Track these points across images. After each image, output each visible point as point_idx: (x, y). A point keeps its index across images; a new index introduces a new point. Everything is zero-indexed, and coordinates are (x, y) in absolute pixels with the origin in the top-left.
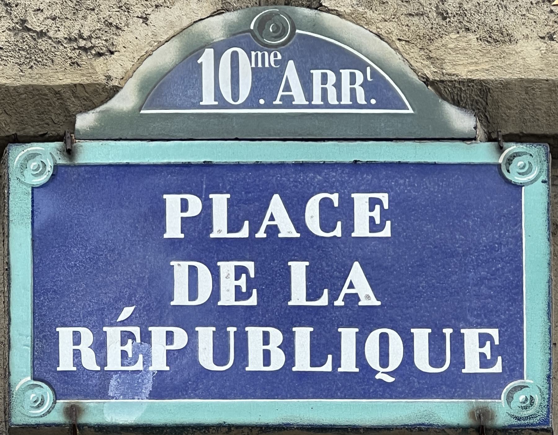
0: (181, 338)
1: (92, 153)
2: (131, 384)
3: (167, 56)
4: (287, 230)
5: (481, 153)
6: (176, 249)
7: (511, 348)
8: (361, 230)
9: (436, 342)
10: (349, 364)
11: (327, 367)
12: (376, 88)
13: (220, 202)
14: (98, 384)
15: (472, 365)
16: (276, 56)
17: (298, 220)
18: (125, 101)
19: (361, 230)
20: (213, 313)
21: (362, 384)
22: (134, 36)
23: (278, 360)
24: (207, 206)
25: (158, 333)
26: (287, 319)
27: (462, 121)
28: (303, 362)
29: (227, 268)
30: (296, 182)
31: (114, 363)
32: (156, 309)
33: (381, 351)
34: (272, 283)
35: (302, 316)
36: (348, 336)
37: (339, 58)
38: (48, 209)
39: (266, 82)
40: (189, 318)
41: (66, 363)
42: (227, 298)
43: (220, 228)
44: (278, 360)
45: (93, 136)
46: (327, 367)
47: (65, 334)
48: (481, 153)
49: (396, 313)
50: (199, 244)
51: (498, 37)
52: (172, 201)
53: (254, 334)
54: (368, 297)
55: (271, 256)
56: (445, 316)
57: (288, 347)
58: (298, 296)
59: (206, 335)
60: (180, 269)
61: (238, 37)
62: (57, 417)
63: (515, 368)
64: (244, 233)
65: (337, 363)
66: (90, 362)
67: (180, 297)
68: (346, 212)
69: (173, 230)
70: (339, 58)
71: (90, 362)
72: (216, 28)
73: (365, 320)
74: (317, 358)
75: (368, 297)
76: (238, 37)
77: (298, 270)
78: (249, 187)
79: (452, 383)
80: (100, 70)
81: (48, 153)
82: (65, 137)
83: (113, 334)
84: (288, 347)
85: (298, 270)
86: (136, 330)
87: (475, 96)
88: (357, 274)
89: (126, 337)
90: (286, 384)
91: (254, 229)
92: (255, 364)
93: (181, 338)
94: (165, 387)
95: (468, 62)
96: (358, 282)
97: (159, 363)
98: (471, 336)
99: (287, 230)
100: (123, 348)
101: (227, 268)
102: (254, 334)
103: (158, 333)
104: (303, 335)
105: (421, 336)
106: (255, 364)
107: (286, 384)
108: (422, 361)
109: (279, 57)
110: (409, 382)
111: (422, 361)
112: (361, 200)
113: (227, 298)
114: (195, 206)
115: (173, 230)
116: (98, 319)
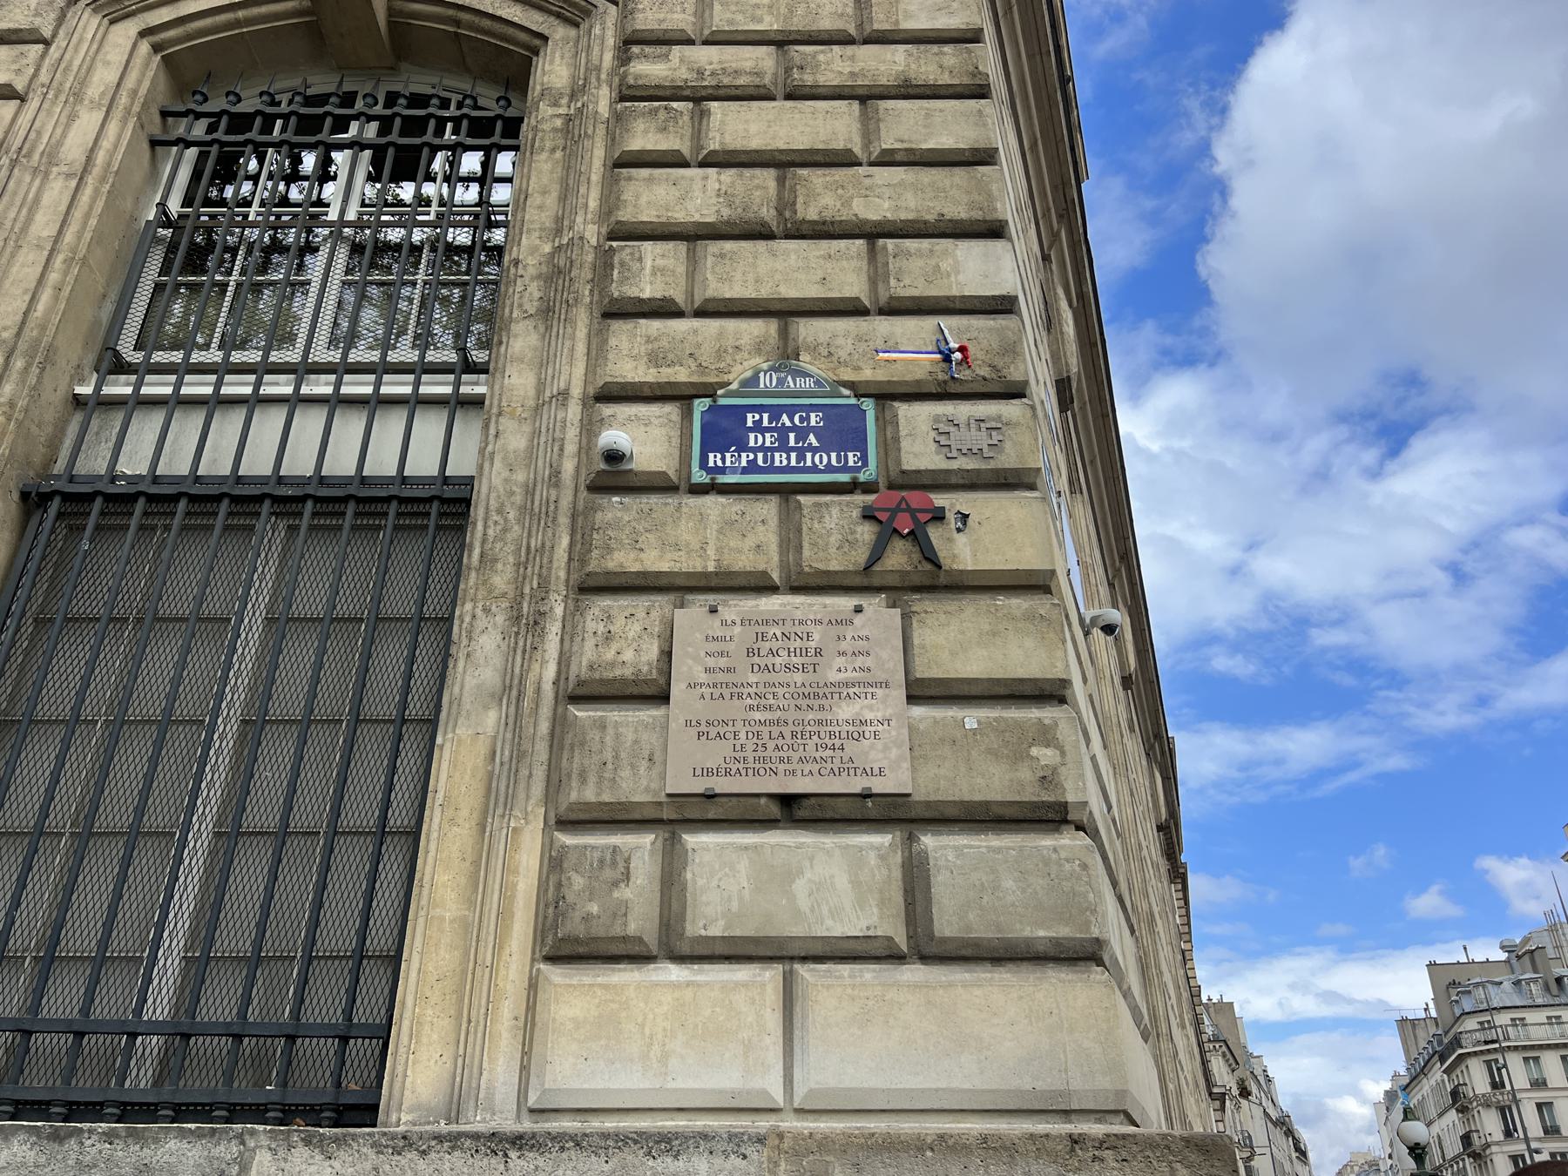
0: (752, 456)
1: (722, 402)
2: (734, 470)
3: (749, 374)
4: (788, 424)
5: (853, 401)
6: (751, 430)
7: (864, 459)
8: (813, 423)
9: (839, 457)
10: (809, 463)
12: (817, 383)
13: (766, 416)
14: (722, 470)
15: (851, 463)
17: (792, 420)
18: (734, 386)
19: (813, 423)
20: (763, 449)
21: (814, 469)
22: (737, 368)
23: (785, 463)
25: (744, 455)
26: (788, 450)
27: (846, 392)
28: (793, 463)
29: (768, 435)
30: (791, 410)
31: (728, 464)
32: (743, 447)
33: (821, 459)
35: (793, 449)
36: (809, 455)
37: (806, 375)
38: (707, 417)
39: (781, 382)
40: (755, 450)
41: (711, 464)
42: (768, 444)
43: (765, 423)
44: (785, 463)
45: (723, 396)
47: (711, 455)
48: (853, 401)
49: (825, 448)
50: (758, 427)
51: (857, 368)
52: (749, 416)
53: (777, 455)
54: (815, 443)
55: (783, 432)
56: (842, 448)
57: (788, 458)
58: (792, 443)
59: (760, 455)
60: (752, 436)
61: (772, 369)
62: (707, 481)
63: (865, 464)
66: (720, 464)
67: (752, 444)
68: (808, 418)
69: (750, 424)
70: (806, 375)
71: (720, 464)
72: (765, 366)
73: (814, 450)
75: (815, 443)
76: (772, 369)
77: (792, 436)
78: (775, 412)
79: (845, 469)
80: (726, 378)
81: (708, 401)
82: (713, 396)
83: (728, 455)
84: (788, 458)
85: (792, 436)
87: (850, 385)
88: (812, 436)
90: (788, 469)
92: (777, 464)
94: (745, 471)
95: (847, 375)
96: (812, 439)
97: (744, 463)
98: (850, 455)
99: (788, 424)
101: (768, 435)
102: (777, 455)
103: (744, 455)
104: (793, 455)
105: (834, 455)
106: (777, 464)
107: (788, 469)
108: (834, 462)
110: (829, 469)
111: (834, 462)
112: (813, 415)
113: (768, 444)
114: (757, 417)
115: (750, 424)
116: (723, 450)
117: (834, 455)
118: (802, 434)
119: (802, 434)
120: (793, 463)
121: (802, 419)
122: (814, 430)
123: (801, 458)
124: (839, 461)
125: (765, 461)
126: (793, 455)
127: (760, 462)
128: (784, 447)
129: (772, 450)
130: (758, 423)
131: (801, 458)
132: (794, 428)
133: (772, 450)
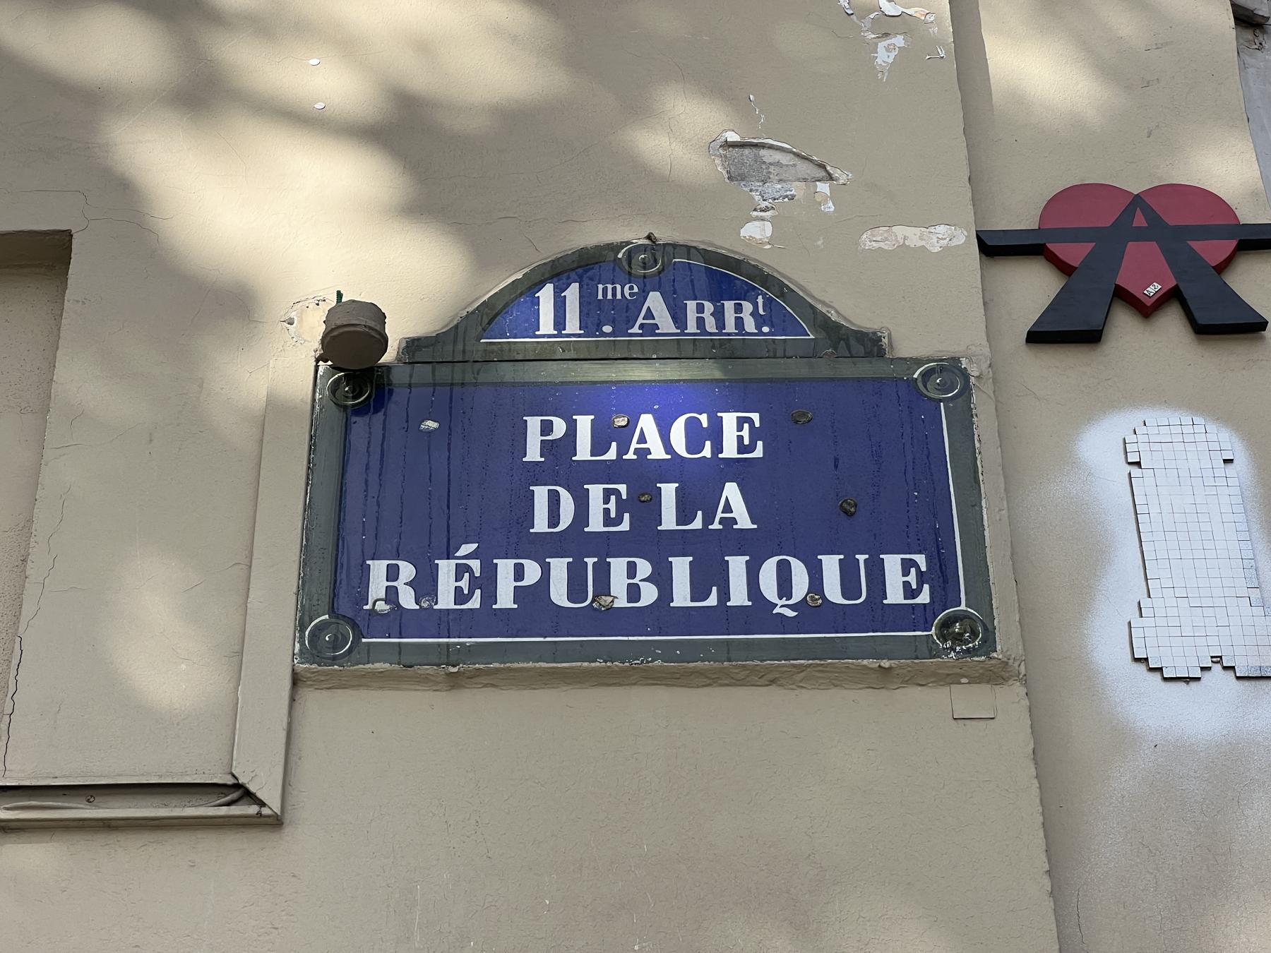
0: (533, 573)
4: (658, 453)
10: (739, 596)
11: (712, 601)
25: (505, 567)
28: (682, 596)
34: (643, 505)
35: (680, 543)
36: (737, 565)
40: (543, 548)
44: (649, 594)
46: (712, 601)
55: (643, 477)
57: (662, 578)
65: (725, 594)
73: (755, 547)
74: (698, 592)
83: (446, 568)
86: (475, 564)
89: (461, 571)
97: (505, 599)
100: (458, 584)
104: (681, 567)
117: (831, 565)
120: (682, 596)
123: (709, 575)
125: (576, 588)
126: (681, 567)
127: (559, 594)
128: (649, 542)
129: (608, 545)
131: (709, 575)
132: (673, 468)
133: (608, 545)
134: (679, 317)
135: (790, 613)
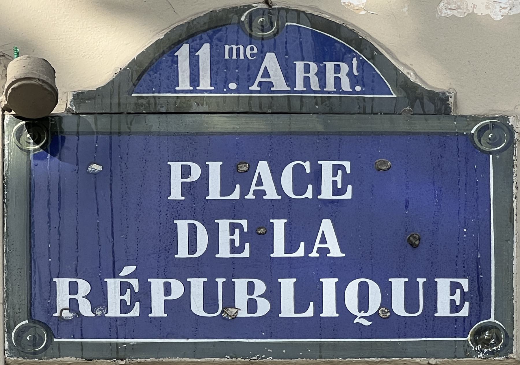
0: (177, 289)
10: (329, 309)
11: (310, 313)
16: (252, 49)
20: (206, 265)
24: (205, 171)
25: (157, 285)
28: (288, 309)
34: (261, 237)
40: (186, 270)
44: (264, 307)
55: (259, 214)
57: (273, 295)
64: (236, 195)
73: (342, 270)
91: (244, 192)
93: (177, 289)
104: (288, 285)
109: (255, 51)
117: (398, 285)
118: (304, 221)
119: (304, 221)
120: (288, 309)
121: (300, 181)
122: (331, 209)
123: (309, 293)
124: (410, 303)
126: (288, 285)
127: (197, 306)
128: (264, 267)
129: (234, 269)
130: (195, 190)
131: (309, 293)
132: (282, 207)
133: (234, 269)
134: (289, 77)
135: (367, 323)
